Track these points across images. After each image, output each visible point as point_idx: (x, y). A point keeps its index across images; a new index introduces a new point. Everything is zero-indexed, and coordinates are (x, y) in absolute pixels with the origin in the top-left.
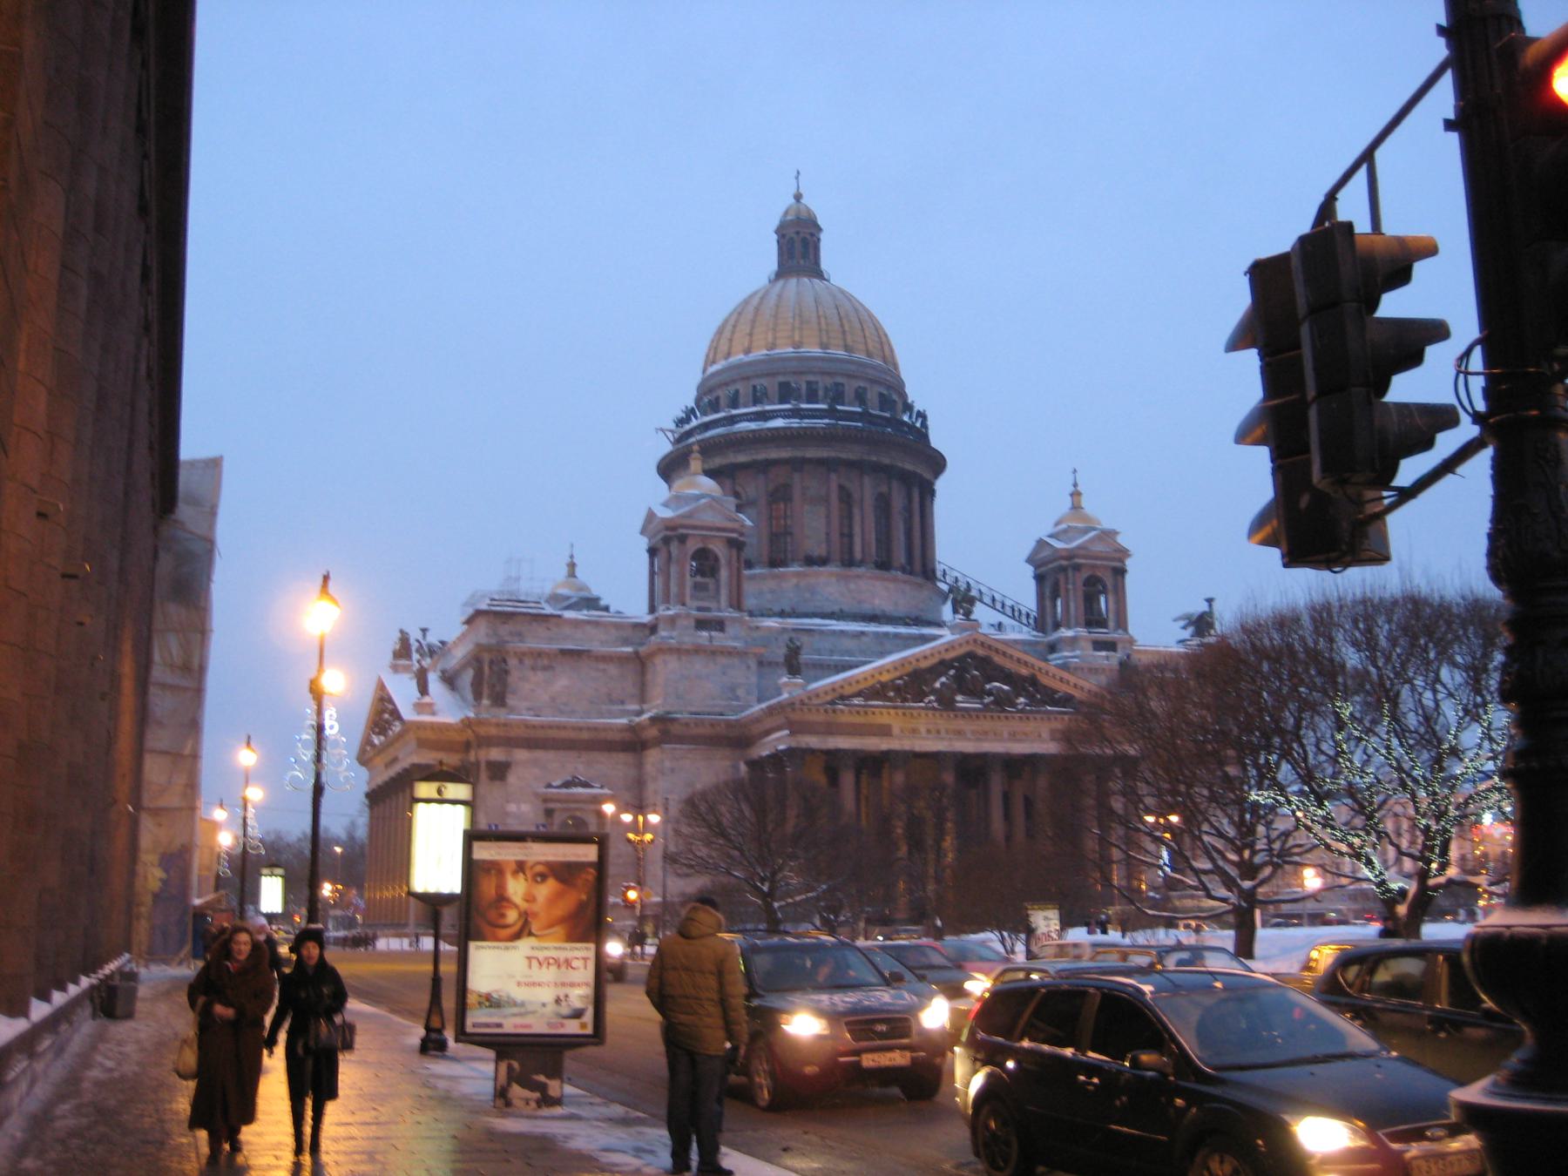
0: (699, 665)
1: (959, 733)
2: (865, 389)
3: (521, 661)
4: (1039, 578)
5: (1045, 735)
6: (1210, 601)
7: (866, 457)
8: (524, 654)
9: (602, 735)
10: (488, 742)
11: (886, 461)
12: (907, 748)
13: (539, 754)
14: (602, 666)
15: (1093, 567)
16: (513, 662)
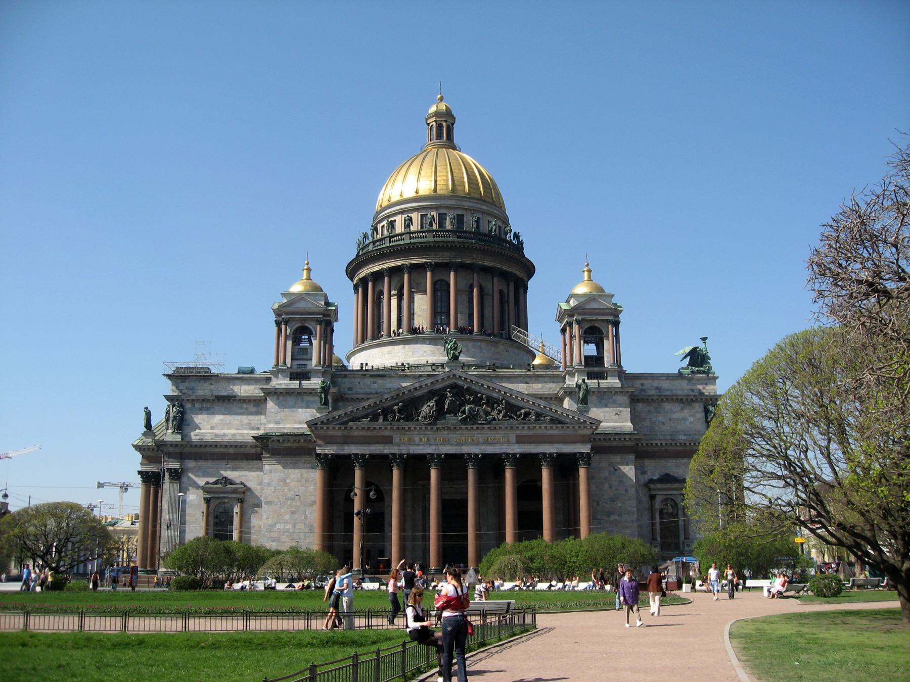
0: (291, 400)
1: (446, 442)
2: (463, 215)
3: (193, 405)
4: (563, 331)
5: (513, 439)
6: (704, 339)
7: (452, 260)
8: (193, 400)
9: (242, 450)
10: (171, 456)
11: (469, 261)
12: (404, 452)
13: (201, 463)
14: (245, 406)
15: (591, 320)
16: (188, 406)
